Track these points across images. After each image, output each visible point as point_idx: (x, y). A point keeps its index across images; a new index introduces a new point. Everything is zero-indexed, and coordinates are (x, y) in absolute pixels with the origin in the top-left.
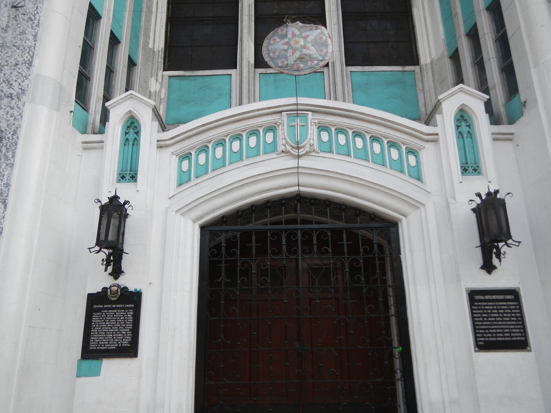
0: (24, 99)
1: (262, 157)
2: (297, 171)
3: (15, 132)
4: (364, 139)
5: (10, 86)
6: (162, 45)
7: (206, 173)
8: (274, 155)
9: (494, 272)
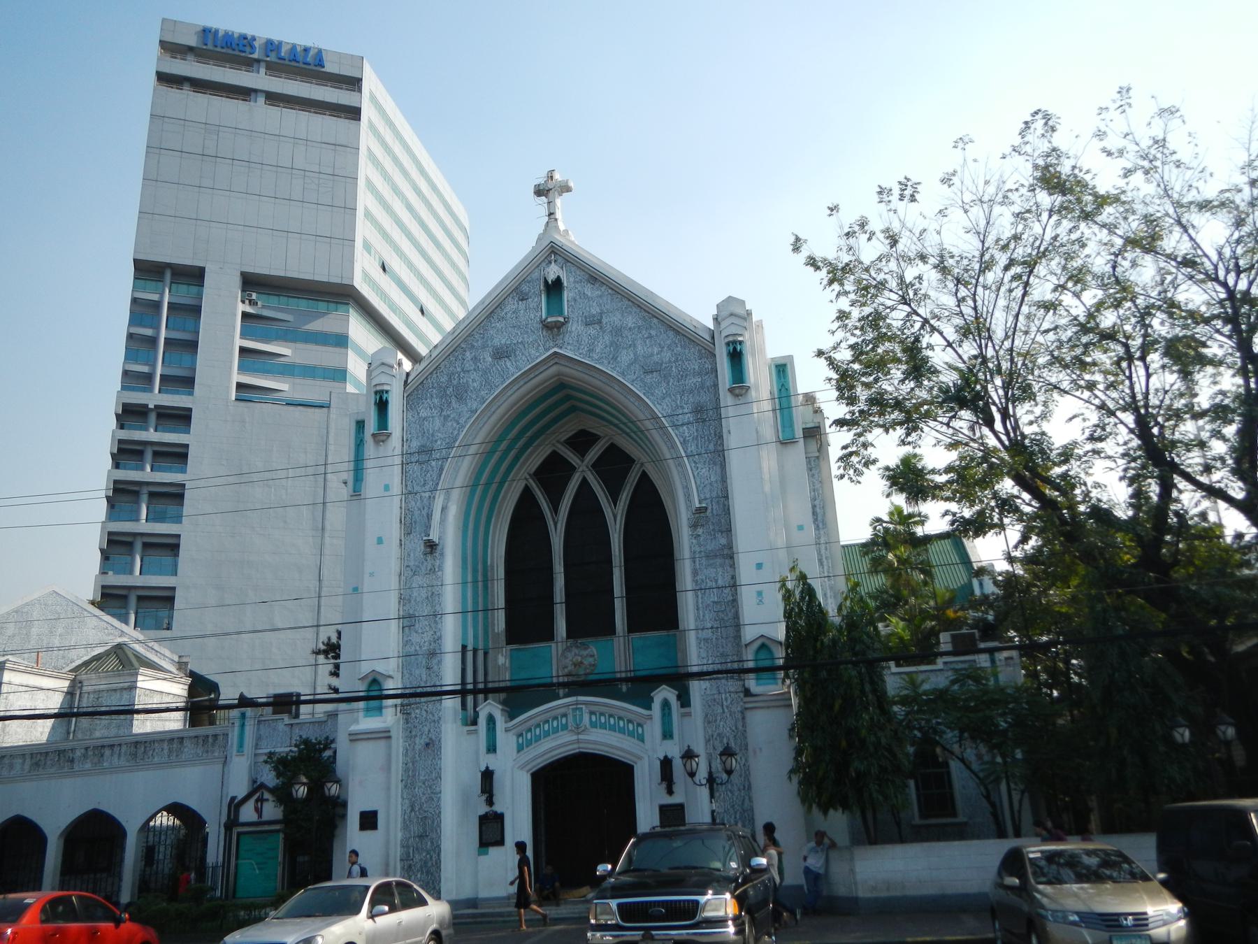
0: (441, 723)
1: (561, 733)
2: (578, 741)
3: (439, 741)
4: (614, 718)
5: (433, 715)
6: (504, 626)
7: (531, 744)
8: (565, 732)
9: (673, 797)
